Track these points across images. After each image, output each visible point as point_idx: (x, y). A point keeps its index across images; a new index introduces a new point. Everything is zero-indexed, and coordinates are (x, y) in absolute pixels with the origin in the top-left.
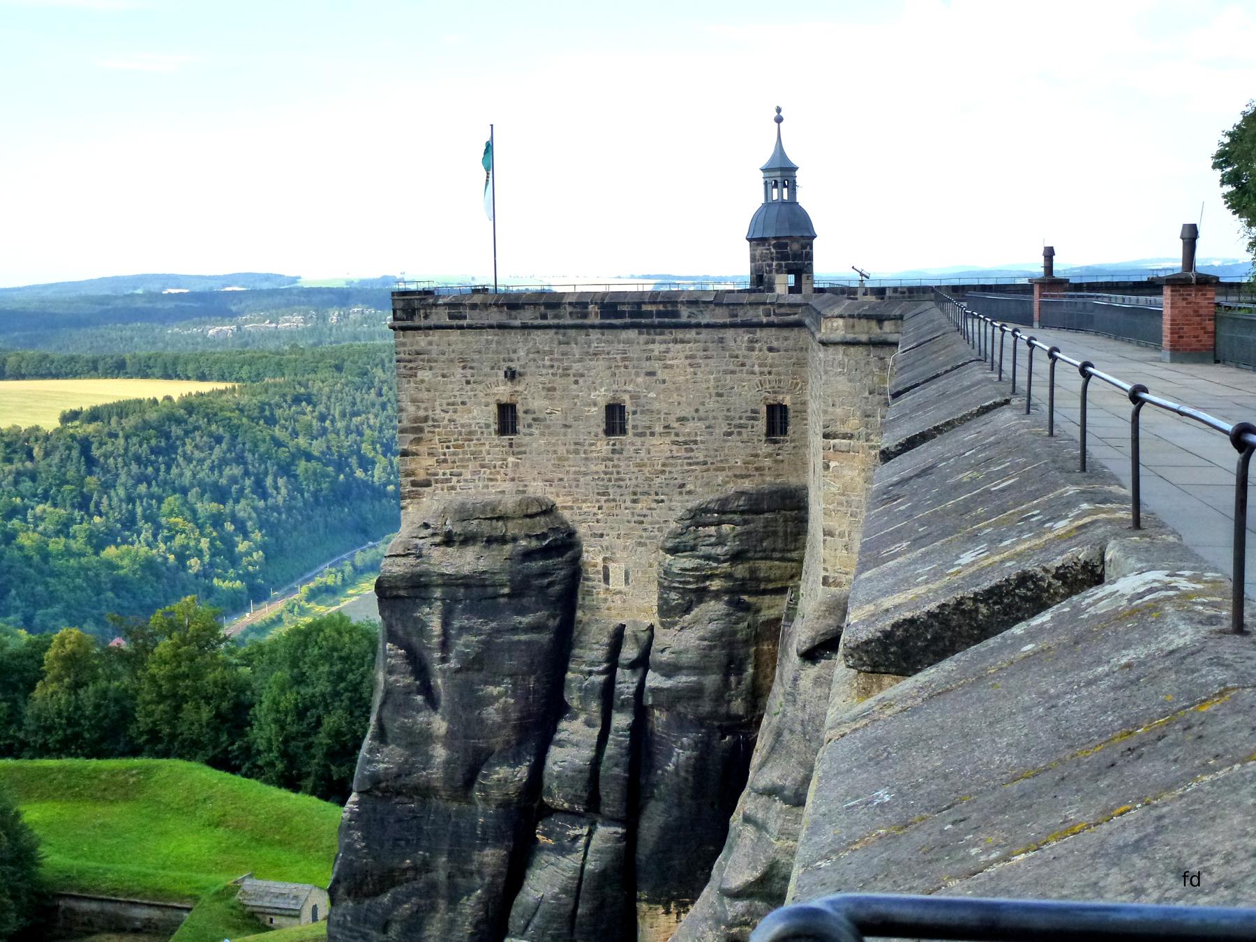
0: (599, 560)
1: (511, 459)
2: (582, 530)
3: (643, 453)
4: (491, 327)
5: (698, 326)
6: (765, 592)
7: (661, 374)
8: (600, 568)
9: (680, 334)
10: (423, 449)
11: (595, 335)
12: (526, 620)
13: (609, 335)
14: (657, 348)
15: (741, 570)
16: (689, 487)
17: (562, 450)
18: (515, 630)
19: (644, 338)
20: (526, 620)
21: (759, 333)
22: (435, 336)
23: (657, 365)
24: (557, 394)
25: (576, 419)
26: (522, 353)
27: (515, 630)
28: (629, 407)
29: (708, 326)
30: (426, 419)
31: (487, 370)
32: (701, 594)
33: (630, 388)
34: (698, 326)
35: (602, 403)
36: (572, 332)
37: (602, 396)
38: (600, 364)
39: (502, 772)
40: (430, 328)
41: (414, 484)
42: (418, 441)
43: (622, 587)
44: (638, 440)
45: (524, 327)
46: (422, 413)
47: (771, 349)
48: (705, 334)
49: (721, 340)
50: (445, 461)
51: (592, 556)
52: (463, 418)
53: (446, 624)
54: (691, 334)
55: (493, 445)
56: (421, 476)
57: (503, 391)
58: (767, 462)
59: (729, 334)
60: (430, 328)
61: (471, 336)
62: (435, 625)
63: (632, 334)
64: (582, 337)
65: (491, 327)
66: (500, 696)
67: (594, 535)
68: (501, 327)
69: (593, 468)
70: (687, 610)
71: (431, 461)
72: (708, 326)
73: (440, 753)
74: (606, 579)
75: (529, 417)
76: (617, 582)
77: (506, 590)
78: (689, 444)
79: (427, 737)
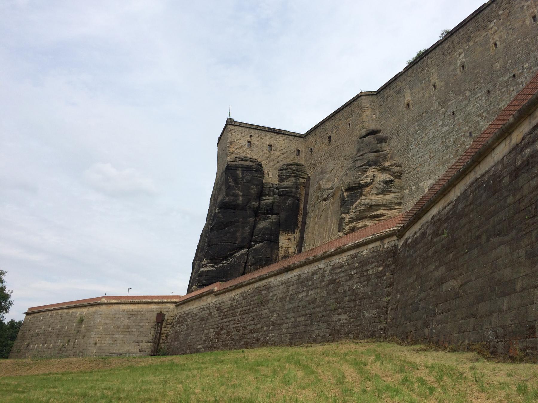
0: (267, 171)
1: (250, 151)
2: (263, 166)
3: (275, 154)
4: (247, 127)
5: (285, 134)
6: (301, 177)
7: (279, 141)
8: (267, 172)
9: (282, 135)
10: (232, 147)
11: (267, 132)
12: (259, 175)
13: (269, 133)
14: (278, 137)
15: (297, 173)
16: (283, 161)
17: (260, 151)
18: (257, 177)
19: (275, 135)
20: (259, 175)
21: (295, 138)
22: (236, 127)
23: (277, 140)
24: (259, 141)
25: (263, 146)
26: (253, 133)
27: (257, 177)
28: (272, 146)
29: (287, 135)
30: (233, 141)
31: (246, 134)
32: (290, 176)
33: (273, 142)
34: (285, 134)
35: (268, 144)
36: (262, 131)
37: (268, 143)
38: (267, 138)
39: (254, 203)
40: (235, 125)
41: (230, 153)
42: (231, 145)
43: (271, 177)
44: (274, 152)
45: (254, 129)
46: (233, 140)
47: (297, 141)
48: (286, 136)
49: (289, 138)
50: (237, 150)
51: (265, 171)
52: (241, 142)
53: (243, 173)
54: (284, 136)
55: (246, 148)
56: (231, 151)
57: (249, 139)
58: (297, 159)
59: (290, 137)
60: (235, 125)
61: (243, 129)
62: (240, 174)
63: (273, 134)
64: (264, 132)
65: (247, 127)
66: (254, 188)
67: (266, 167)
68: (249, 128)
69: (265, 155)
70: (287, 179)
71: (234, 149)
72: (287, 135)
73: (241, 198)
74: (268, 175)
75: (254, 144)
76: (270, 176)
77: (255, 170)
78: (283, 154)
79: (238, 195)
